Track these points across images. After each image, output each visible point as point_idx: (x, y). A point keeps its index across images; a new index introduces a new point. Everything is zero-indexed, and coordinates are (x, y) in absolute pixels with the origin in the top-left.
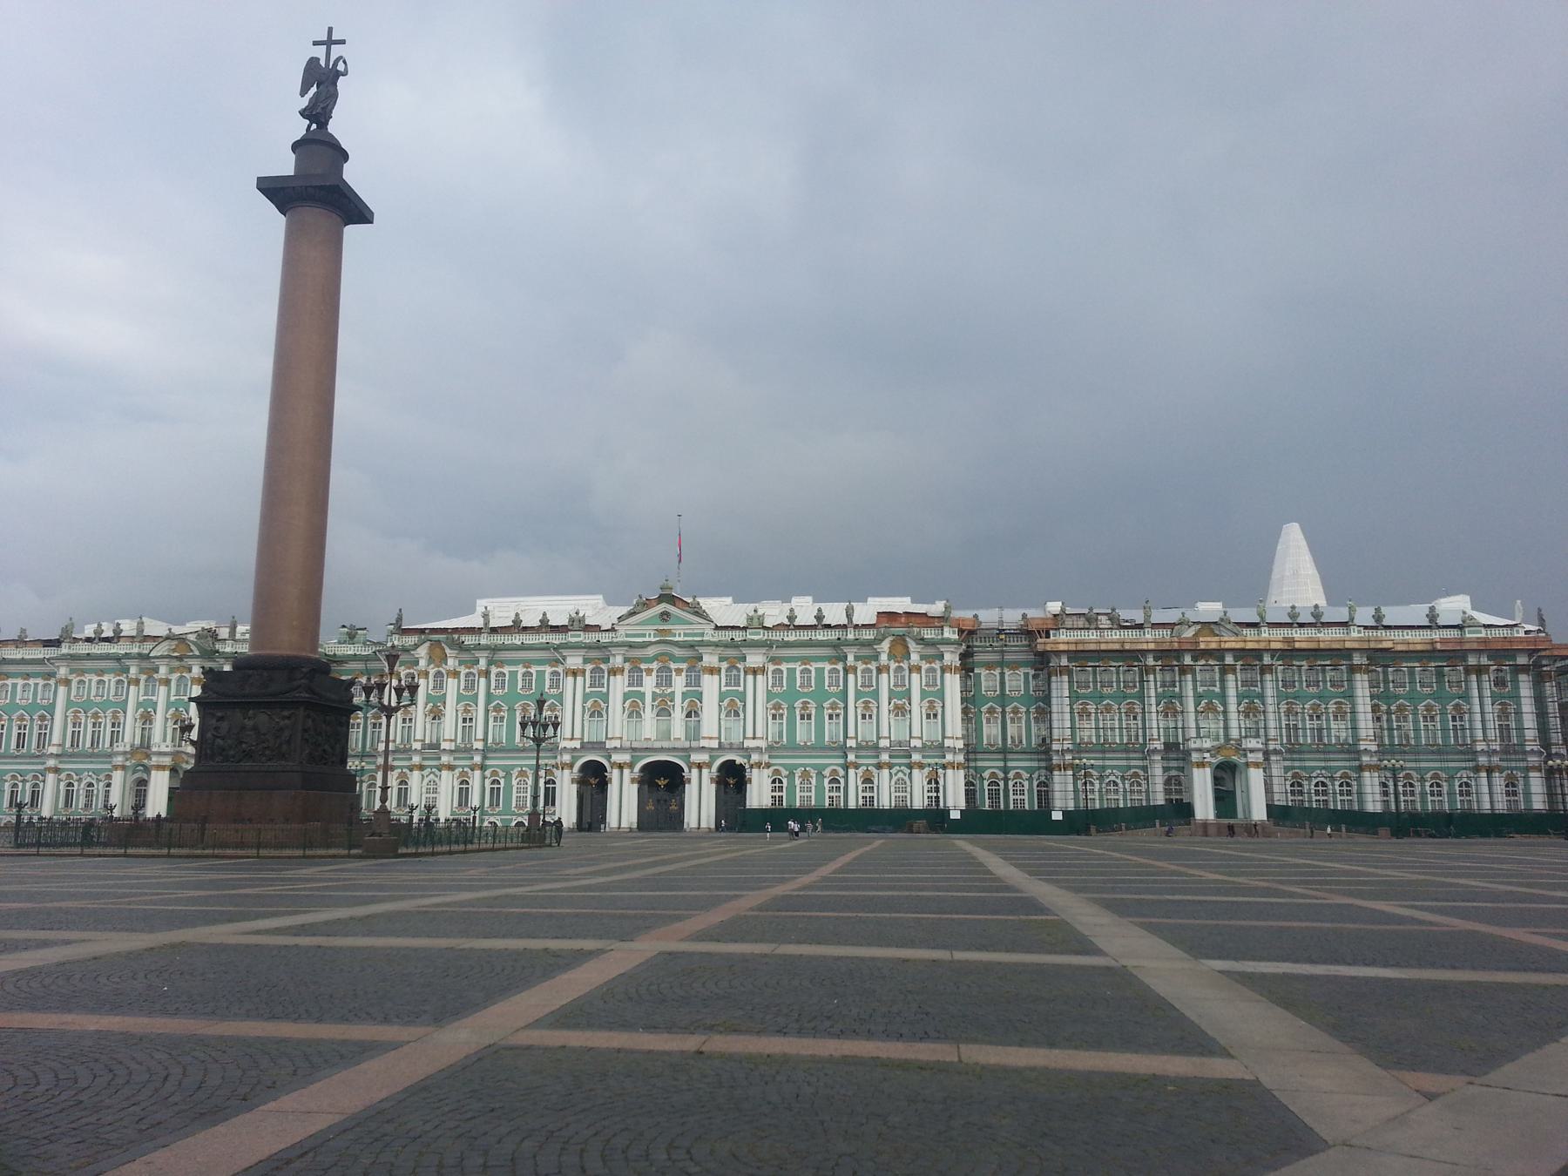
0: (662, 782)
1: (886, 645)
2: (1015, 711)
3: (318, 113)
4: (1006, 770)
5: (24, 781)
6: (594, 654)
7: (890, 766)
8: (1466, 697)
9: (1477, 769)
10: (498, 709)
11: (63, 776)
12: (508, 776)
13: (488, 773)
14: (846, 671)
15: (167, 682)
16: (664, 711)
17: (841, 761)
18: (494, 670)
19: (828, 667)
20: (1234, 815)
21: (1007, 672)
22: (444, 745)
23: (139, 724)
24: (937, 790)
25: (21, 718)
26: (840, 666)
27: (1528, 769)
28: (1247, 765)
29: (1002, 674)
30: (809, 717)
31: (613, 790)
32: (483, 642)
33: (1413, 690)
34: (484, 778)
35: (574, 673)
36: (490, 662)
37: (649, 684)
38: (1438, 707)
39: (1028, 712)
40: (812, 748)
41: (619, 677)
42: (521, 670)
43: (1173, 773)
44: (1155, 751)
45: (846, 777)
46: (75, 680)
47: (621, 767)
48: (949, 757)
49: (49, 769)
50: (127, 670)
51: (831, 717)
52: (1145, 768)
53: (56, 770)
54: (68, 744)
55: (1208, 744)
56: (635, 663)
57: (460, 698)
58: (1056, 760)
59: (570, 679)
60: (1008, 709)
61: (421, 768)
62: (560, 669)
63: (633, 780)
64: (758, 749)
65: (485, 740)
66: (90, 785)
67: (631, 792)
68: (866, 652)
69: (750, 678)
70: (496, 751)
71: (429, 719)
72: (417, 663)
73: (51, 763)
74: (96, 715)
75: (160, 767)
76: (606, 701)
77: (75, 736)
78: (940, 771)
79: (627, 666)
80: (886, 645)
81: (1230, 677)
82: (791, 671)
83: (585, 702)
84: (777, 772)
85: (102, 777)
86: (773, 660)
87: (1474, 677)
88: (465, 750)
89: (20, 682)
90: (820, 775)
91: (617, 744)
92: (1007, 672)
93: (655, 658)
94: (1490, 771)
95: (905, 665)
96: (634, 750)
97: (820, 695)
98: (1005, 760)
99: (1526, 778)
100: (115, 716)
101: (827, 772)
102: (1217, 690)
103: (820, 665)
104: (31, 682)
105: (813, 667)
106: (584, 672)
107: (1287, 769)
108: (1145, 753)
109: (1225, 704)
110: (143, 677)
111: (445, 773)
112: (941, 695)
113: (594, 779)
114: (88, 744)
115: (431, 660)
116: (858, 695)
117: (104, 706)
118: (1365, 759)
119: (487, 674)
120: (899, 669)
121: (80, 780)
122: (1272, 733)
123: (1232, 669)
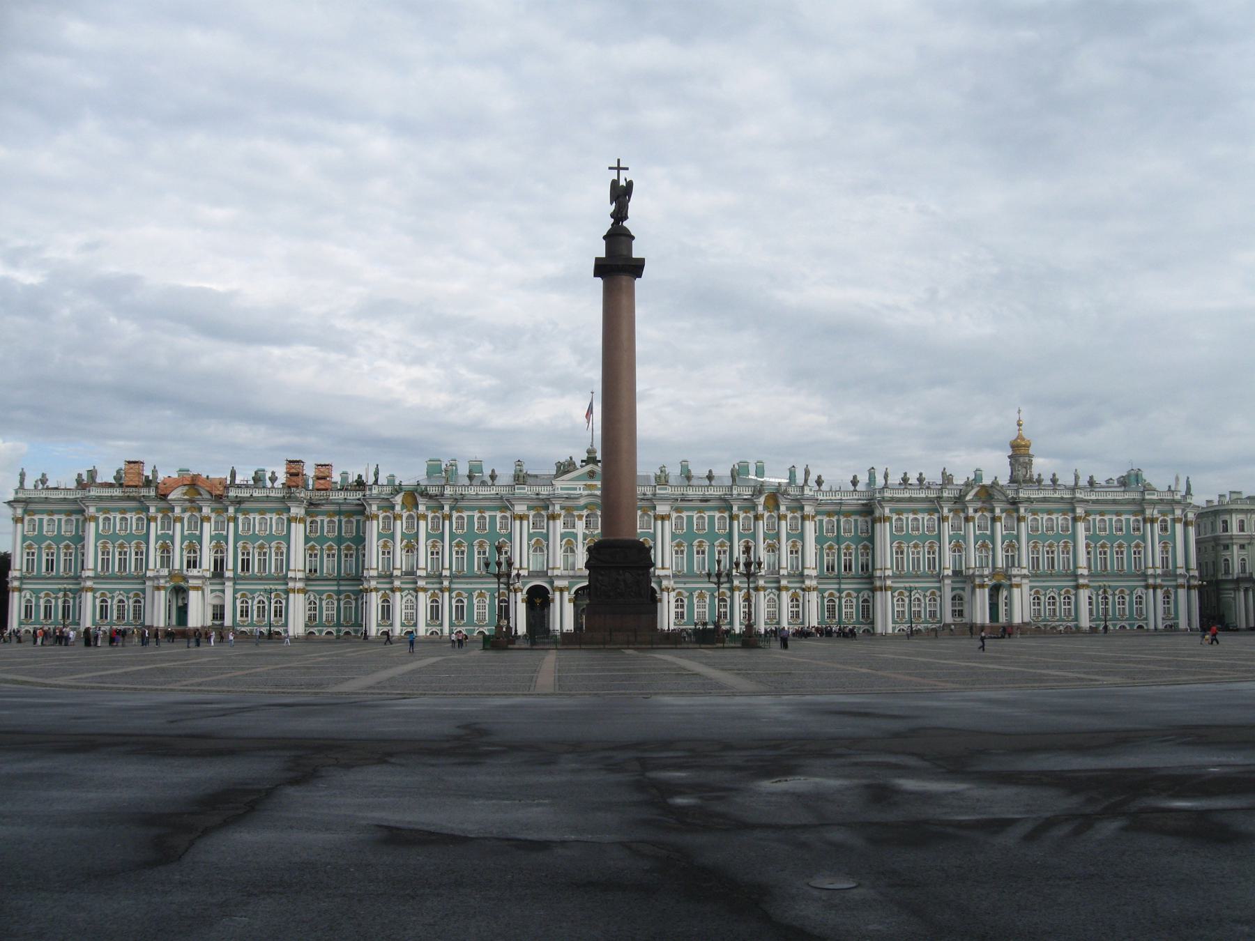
2: (848, 548)
4: (840, 591)
5: (56, 598)
7: (765, 589)
8: (1144, 538)
9: (1147, 587)
10: (459, 545)
11: (98, 594)
13: (454, 594)
14: (732, 518)
15: (181, 520)
18: (455, 514)
19: (717, 515)
20: (997, 621)
21: (843, 520)
22: (420, 573)
23: (159, 553)
24: (798, 606)
25: (49, 547)
26: (726, 515)
27: (1177, 587)
29: (838, 521)
30: (703, 552)
31: (555, 608)
34: (450, 598)
36: (452, 509)
39: (857, 549)
42: (477, 515)
43: (958, 592)
44: (948, 576)
45: (732, 598)
46: (101, 517)
47: (561, 590)
48: (808, 583)
52: (939, 589)
53: (92, 589)
55: (986, 572)
56: (568, 509)
57: (428, 536)
58: (878, 583)
59: (518, 522)
60: (843, 546)
61: (401, 590)
62: (508, 514)
63: (570, 600)
64: (667, 577)
66: (121, 601)
67: (569, 609)
69: (659, 522)
70: (457, 577)
71: (404, 552)
72: (393, 507)
73: (89, 584)
75: (196, 588)
77: (106, 563)
78: (801, 593)
80: (762, 499)
81: (998, 525)
82: (690, 518)
83: (529, 540)
84: (679, 594)
85: (131, 595)
86: (678, 510)
89: (46, 518)
91: (556, 572)
92: (843, 520)
94: (1155, 587)
97: (712, 536)
98: (839, 583)
99: (1176, 593)
100: (138, 546)
102: (988, 533)
103: (711, 513)
104: (56, 517)
105: (706, 515)
106: (527, 517)
107: (1031, 588)
108: (940, 578)
109: (993, 543)
110: (160, 516)
111: (421, 595)
112: (802, 536)
113: (539, 600)
115: (404, 505)
118: (1081, 581)
119: (450, 517)
120: (771, 516)
121: (112, 598)
122: (1024, 564)
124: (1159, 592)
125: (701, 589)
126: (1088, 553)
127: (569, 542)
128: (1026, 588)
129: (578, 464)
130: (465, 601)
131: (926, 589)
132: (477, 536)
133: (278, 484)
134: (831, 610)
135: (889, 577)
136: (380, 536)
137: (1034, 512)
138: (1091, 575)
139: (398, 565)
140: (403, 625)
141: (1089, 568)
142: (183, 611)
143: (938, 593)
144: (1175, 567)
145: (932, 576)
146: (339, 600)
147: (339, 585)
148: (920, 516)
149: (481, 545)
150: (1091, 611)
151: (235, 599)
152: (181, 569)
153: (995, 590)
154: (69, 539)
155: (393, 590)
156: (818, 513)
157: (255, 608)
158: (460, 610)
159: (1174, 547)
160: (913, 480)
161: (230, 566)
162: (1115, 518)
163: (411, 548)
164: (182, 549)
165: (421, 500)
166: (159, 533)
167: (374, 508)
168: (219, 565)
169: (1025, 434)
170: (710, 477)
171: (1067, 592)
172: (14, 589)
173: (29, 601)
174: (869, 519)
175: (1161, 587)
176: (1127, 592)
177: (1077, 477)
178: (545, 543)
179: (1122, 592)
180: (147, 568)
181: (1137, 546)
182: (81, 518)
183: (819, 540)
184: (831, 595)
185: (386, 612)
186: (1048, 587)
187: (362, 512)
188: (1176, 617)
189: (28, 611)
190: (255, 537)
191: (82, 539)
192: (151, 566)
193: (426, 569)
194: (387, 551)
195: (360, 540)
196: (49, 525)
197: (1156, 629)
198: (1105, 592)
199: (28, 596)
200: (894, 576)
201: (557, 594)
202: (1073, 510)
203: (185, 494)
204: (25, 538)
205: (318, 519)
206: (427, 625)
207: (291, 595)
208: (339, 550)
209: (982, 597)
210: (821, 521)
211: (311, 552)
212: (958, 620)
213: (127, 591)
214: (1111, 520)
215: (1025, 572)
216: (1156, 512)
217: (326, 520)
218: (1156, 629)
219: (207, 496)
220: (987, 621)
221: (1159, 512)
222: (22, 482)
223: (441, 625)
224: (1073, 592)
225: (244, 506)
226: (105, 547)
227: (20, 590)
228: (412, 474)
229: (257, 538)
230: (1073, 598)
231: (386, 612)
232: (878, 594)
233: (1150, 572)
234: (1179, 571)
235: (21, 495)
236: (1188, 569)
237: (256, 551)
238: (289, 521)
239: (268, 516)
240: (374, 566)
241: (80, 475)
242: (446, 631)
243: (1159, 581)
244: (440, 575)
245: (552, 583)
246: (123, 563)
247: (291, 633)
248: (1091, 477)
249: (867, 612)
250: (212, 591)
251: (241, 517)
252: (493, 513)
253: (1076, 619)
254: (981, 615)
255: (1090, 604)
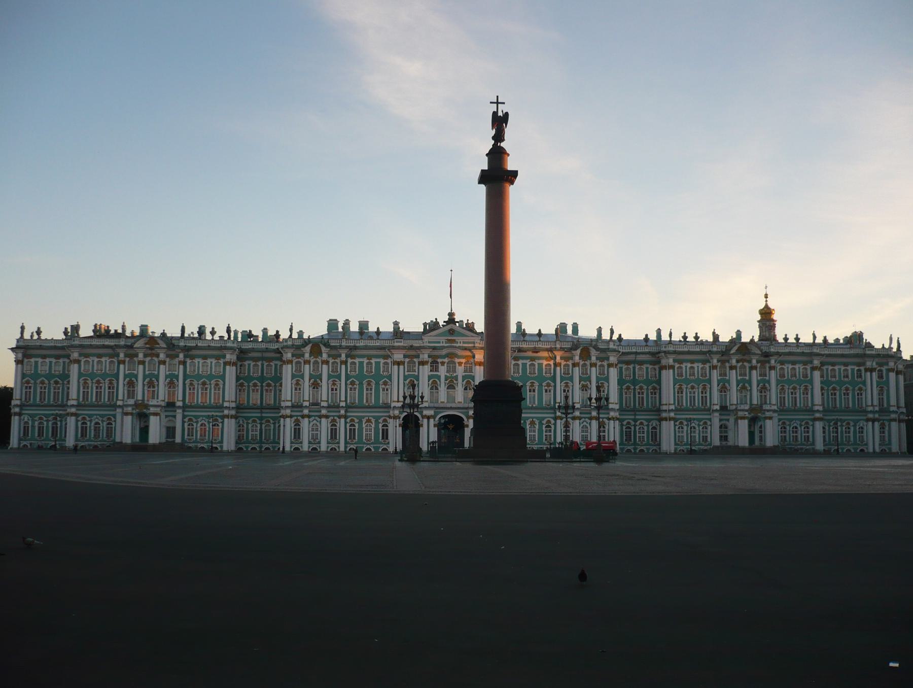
0: (451, 427)
1: (578, 351)
2: (641, 388)
3: (499, 137)
4: (635, 420)
5: (48, 421)
6: (413, 353)
7: (580, 418)
8: (864, 383)
9: (868, 420)
10: (353, 383)
11: (80, 418)
12: (360, 422)
13: (348, 420)
14: (556, 365)
15: (143, 363)
16: (451, 387)
17: (553, 415)
18: (350, 361)
21: (637, 367)
28: (766, 418)
29: (634, 368)
30: (534, 391)
31: (423, 431)
32: (344, 344)
33: (849, 383)
34: (346, 423)
35: (399, 364)
36: (347, 356)
37: (443, 371)
38: (851, 388)
40: (536, 408)
41: (426, 367)
43: (724, 422)
44: (716, 410)
45: (555, 424)
46: (83, 360)
47: (428, 418)
49: (72, 414)
50: (118, 355)
51: (546, 391)
52: (710, 420)
54: (81, 399)
57: (329, 377)
59: (396, 367)
61: (309, 416)
62: (389, 361)
63: (435, 426)
65: (346, 401)
66: (97, 423)
68: (567, 355)
72: (303, 355)
73: (73, 410)
74: (98, 382)
75: (156, 414)
76: (418, 380)
79: (430, 360)
80: (578, 351)
82: (524, 365)
83: (405, 380)
85: (105, 419)
87: (869, 374)
88: (333, 407)
89: (40, 360)
90: (541, 424)
93: (447, 356)
94: (873, 421)
95: (588, 363)
96: (437, 408)
99: (889, 425)
100: (111, 382)
101: (544, 422)
102: (747, 378)
104: (47, 360)
106: (403, 363)
107: (779, 420)
108: (709, 411)
109: (751, 386)
111: (323, 420)
112: (607, 379)
113: (411, 425)
114: (94, 399)
115: (311, 353)
116: (562, 379)
117: (104, 376)
118: (818, 415)
119: (345, 363)
120: (584, 365)
121: (91, 421)
122: (774, 402)
123: (755, 368)
124: (877, 424)
125: (533, 418)
126: (823, 394)
127: (434, 382)
128: (776, 420)
129: (441, 323)
130: (357, 425)
131: (699, 420)
132: (367, 377)
133: (216, 337)
134: (628, 434)
135: (672, 410)
136: (293, 376)
137: (782, 363)
138: (826, 411)
139: (306, 398)
140: (310, 443)
141: (823, 404)
142: (145, 431)
143: (709, 423)
144: (889, 405)
145: (704, 410)
146: (261, 424)
147: (262, 413)
148: (695, 365)
149: (369, 384)
150: (824, 437)
151: (183, 422)
152: (143, 400)
153: (753, 421)
154: (58, 376)
155: (303, 417)
156: (620, 362)
157: (198, 429)
158: (352, 432)
159: (888, 390)
160: (691, 338)
161: (180, 398)
162: (843, 368)
163: (316, 385)
164: (144, 385)
165: (323, 349)
166: (127, 372)
167: (289, 355)
168: (171, 394)
169: (771, 306)
170: (540, 334)
171: (807, 423)
172: (16, 414)
173: (26, 423)
174: (657, 367)
175: (878, 420)
176: (852, 424)
177: (815, 337)
178: (416, 382)
179: (848, 424)
180: (117, 399)
181: (860, 389)
182: (67, 361)
183: (621, 382)
184: (628, 423)
185: (297, 433)
186: (793, 419)
187: (280, 359)
188: (890, 443)
189: (26, 430)
190: (198, 377)
191: (68, 376)
192: (120, 397)
193: (327, 401)
194: (298, 386)
195: (278, 379)
196: (44, 366)
197: (874, 451)
198: (836, 424)
199: (26, 419)
200: (676, 410)
201: (425, 421)
202: (811, 362)
203: (146, 344)
204: (24, 376)
205: (246, 363)
206: (328, 443)
207: (226, 420)
208: (262, 386)
209: (744, 425)
210: (621, 368)
211: (240, 387)
212: (724, 443)
213: (102, 416)
214: (840, 369)
215: (775, 408)
216: (874, 364)
217: (252, 364)
218: (874, 451)
219: (165, 346)
220: (747, 445)
221: (877, 364)
222: (22, 333)
223: (338, 443)
224: (811, 423)
225: (190, 353)
226: (85, 383)
227: (20, 414)
228: (316, 329)
229: (202, 377)
230: (811, 428)
231: (297, 433)
232: (664, 423)
233: (870, 409)
234: (892, 409)
235: (21, 344)
236: (898, 407)
237: (200, 386)
238: (225, 364)
239: (209, 361)
240: (289, 398)
241: (66, 329)
242: (342, 449)
243: (877, 416)
244: (338, 407)
245: (421, 413)
246: (98, 394)
247: (225, 448)
248: (825, 337)
249: (655, 437)
250: (166, 416)
251: (188, 361)
252: (378, 360)
253: (813, 444)
254: (743, 440)
255: (824, 432)
